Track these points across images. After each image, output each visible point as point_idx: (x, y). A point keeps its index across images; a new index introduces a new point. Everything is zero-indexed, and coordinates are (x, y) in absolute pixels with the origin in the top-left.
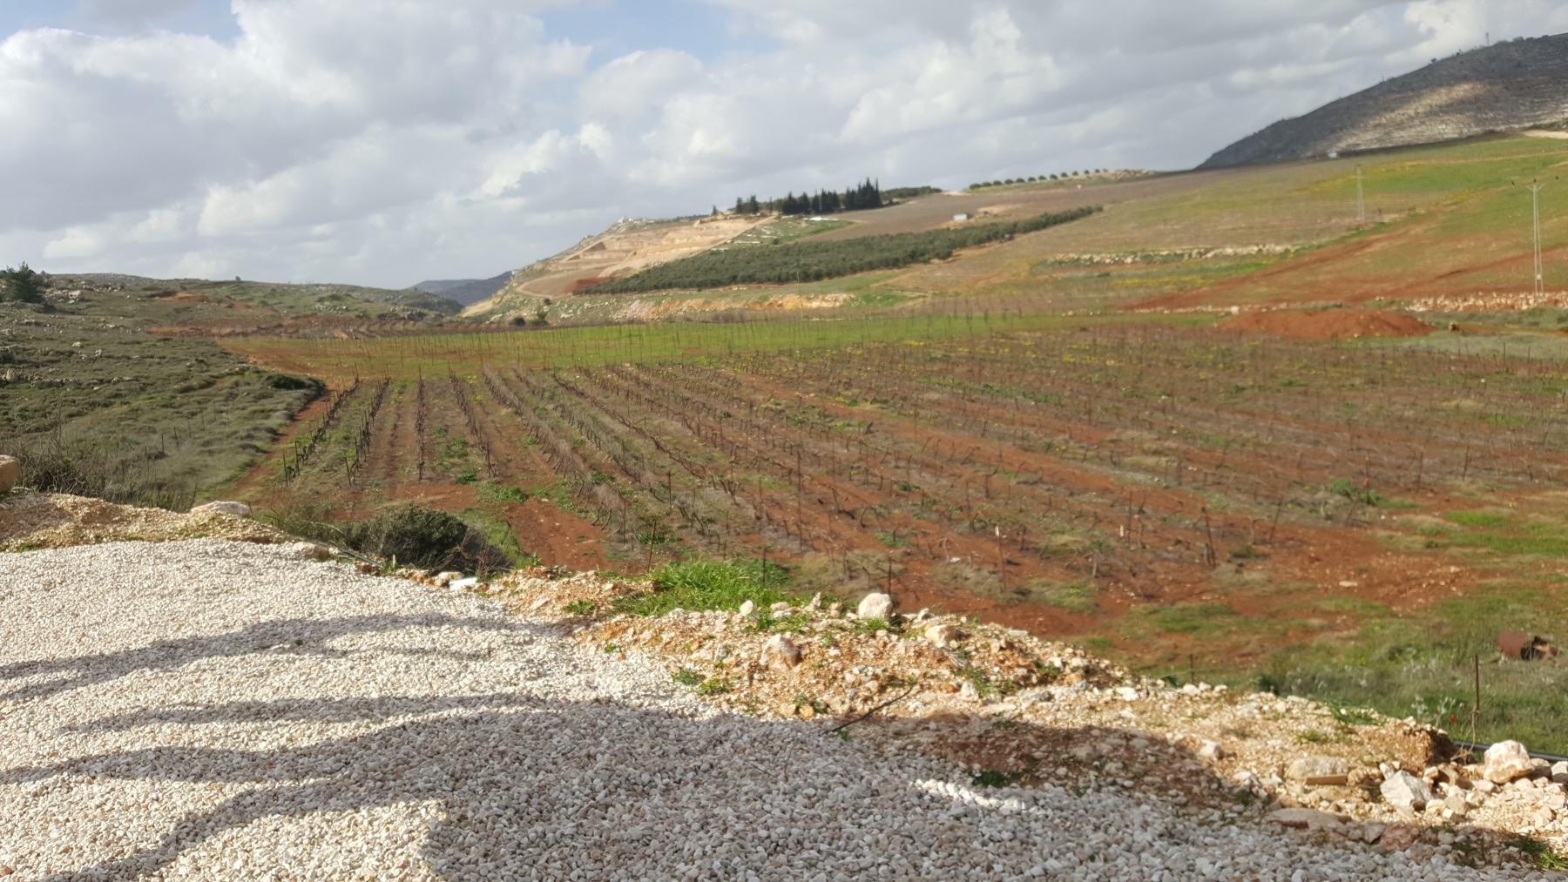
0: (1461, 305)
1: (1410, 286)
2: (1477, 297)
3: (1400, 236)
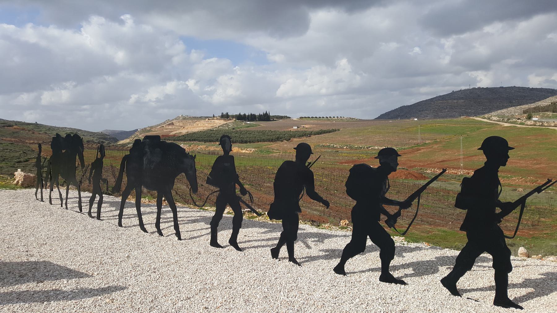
1: (428, 164)
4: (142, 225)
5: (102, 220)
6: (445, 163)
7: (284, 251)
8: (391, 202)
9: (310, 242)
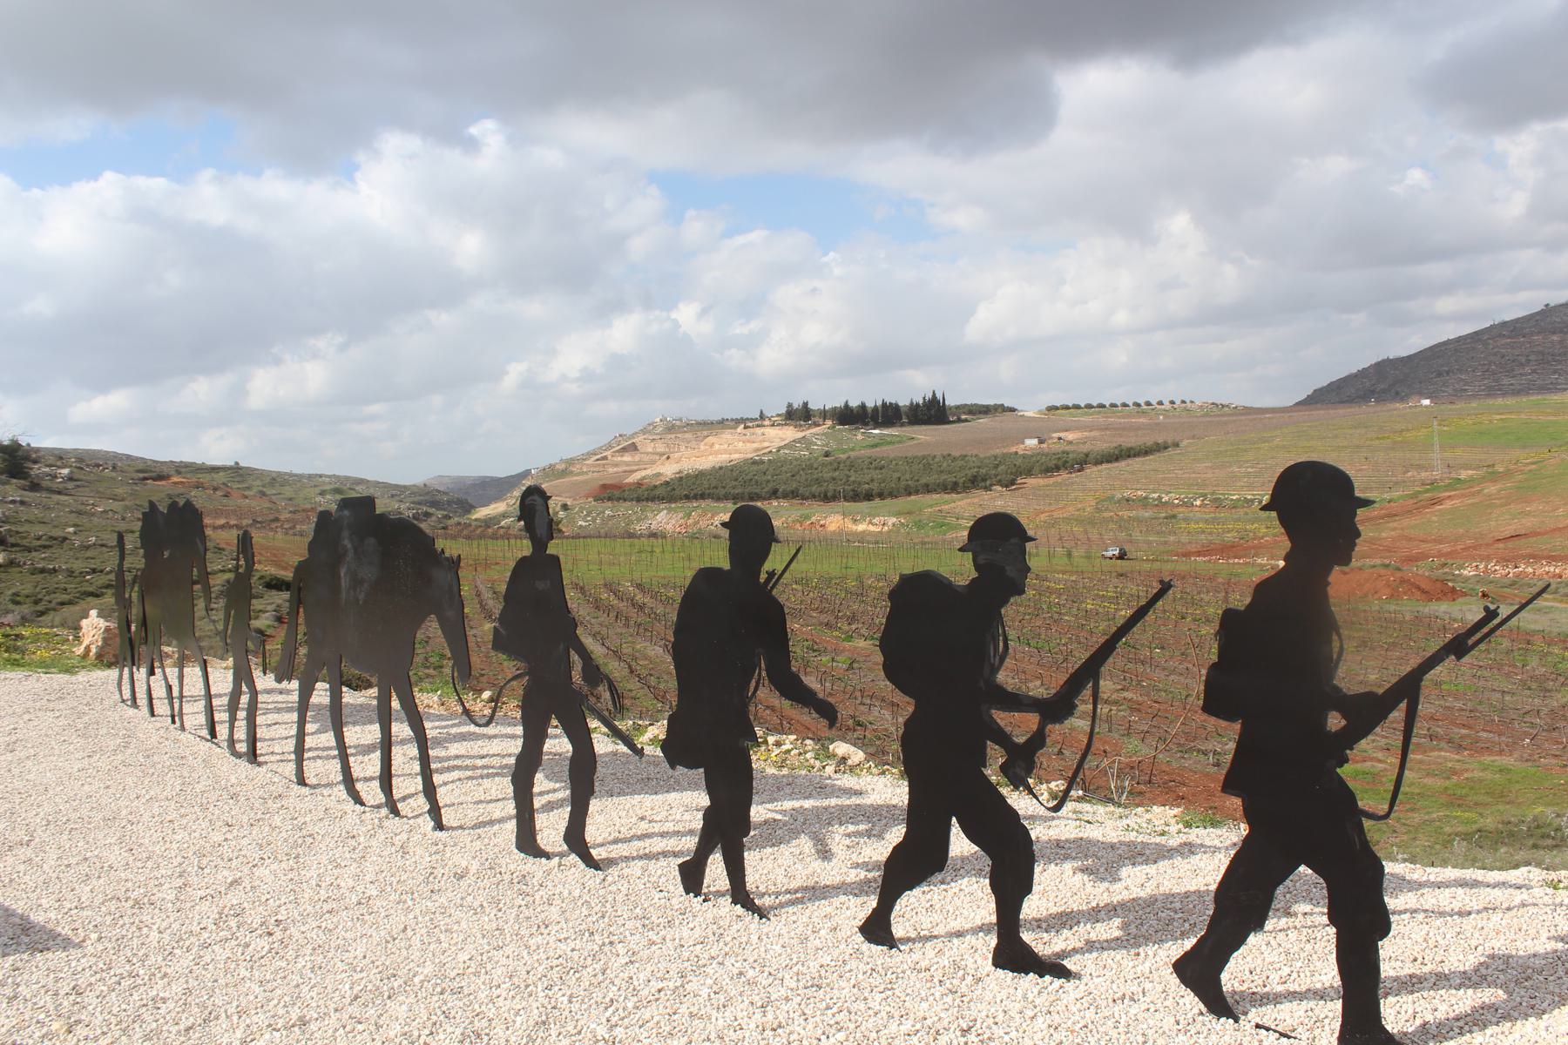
0: (1512, 572)
2: (1528, 564)
3: (1473, 494)
4: (349, 781)
5: (260, 764)
6: (1523, 541)
7: (716, 871)
8: (1015, 702)
9: (837, 838)
